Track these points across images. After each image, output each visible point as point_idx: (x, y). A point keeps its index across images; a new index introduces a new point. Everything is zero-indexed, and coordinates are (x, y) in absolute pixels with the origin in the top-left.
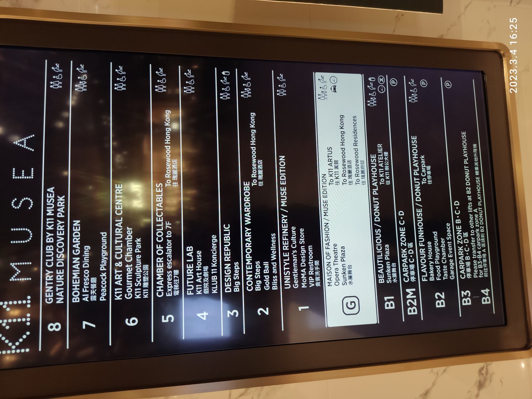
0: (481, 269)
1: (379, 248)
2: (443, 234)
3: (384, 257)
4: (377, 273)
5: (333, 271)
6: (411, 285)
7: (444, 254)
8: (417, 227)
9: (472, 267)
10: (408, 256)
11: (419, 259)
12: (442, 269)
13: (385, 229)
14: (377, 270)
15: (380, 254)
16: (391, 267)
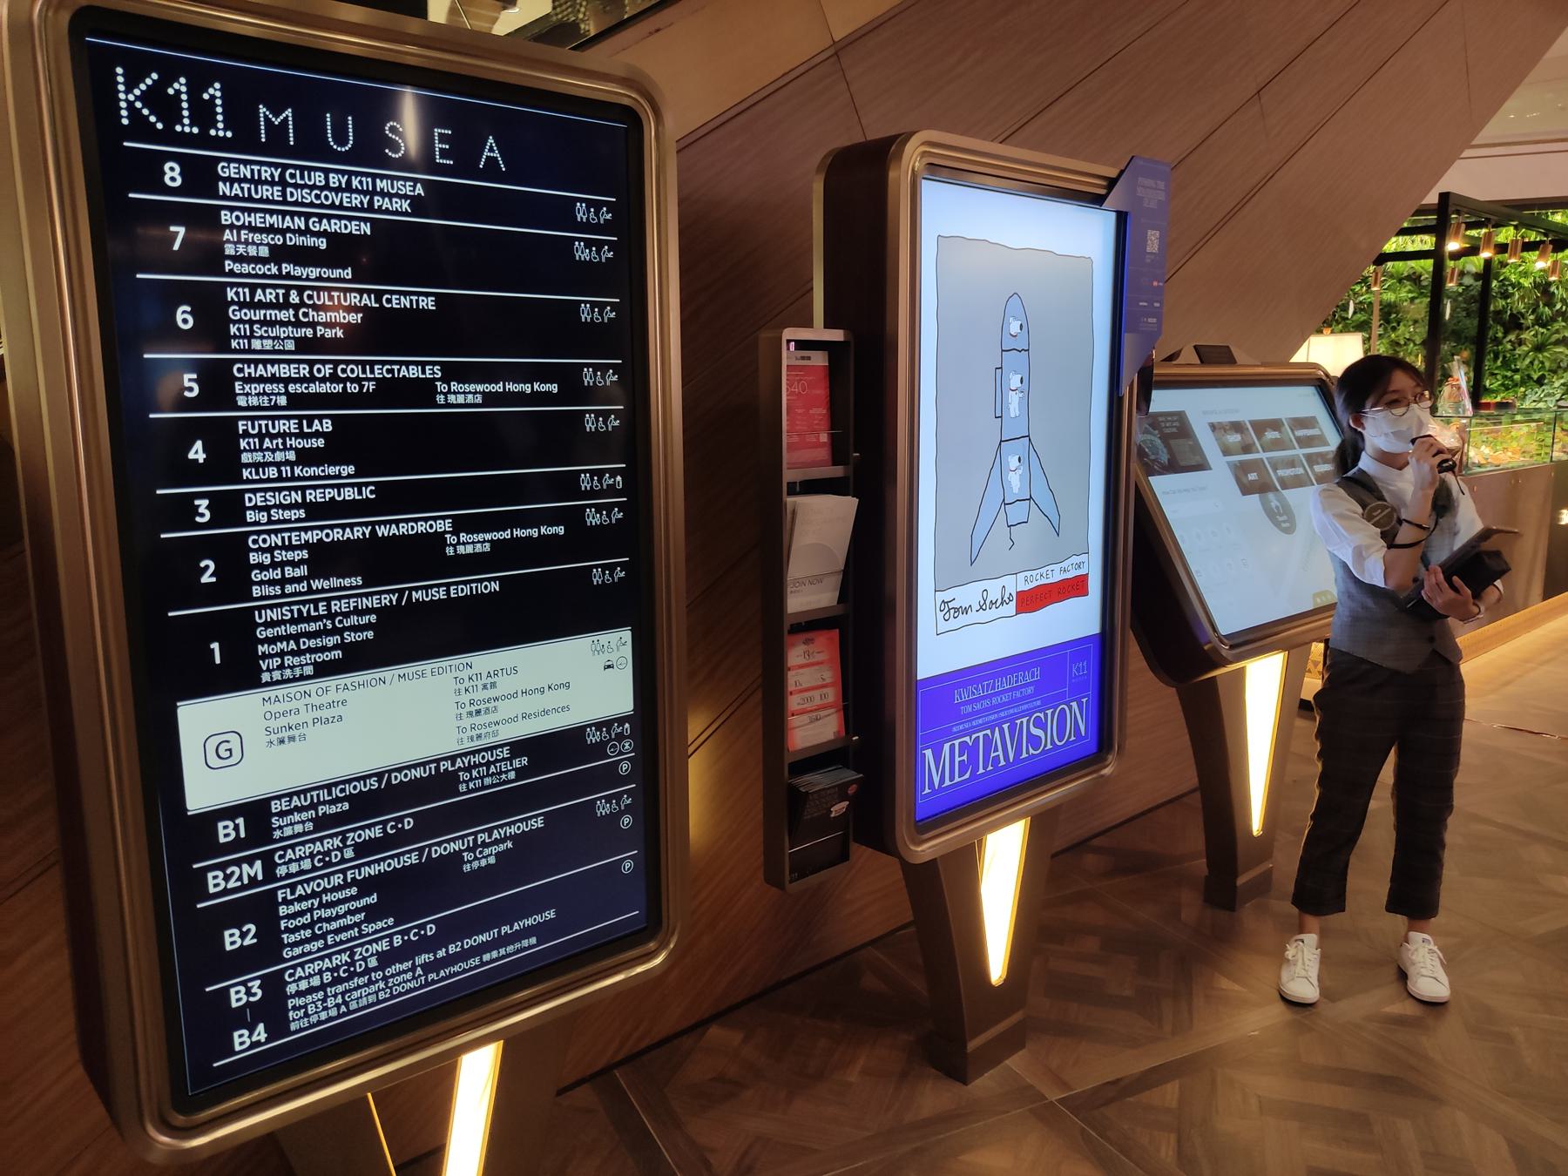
1: (342, 791)
2: (372, 914)
3: (324, 803)
4: (290, 795)
5: (294, 705)
8: (384, 859)
11: (322, 877)
14: (298, 793)
15: (330, 794)
16: (303, 822)
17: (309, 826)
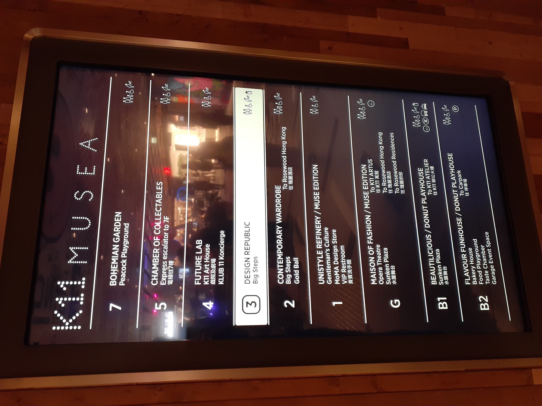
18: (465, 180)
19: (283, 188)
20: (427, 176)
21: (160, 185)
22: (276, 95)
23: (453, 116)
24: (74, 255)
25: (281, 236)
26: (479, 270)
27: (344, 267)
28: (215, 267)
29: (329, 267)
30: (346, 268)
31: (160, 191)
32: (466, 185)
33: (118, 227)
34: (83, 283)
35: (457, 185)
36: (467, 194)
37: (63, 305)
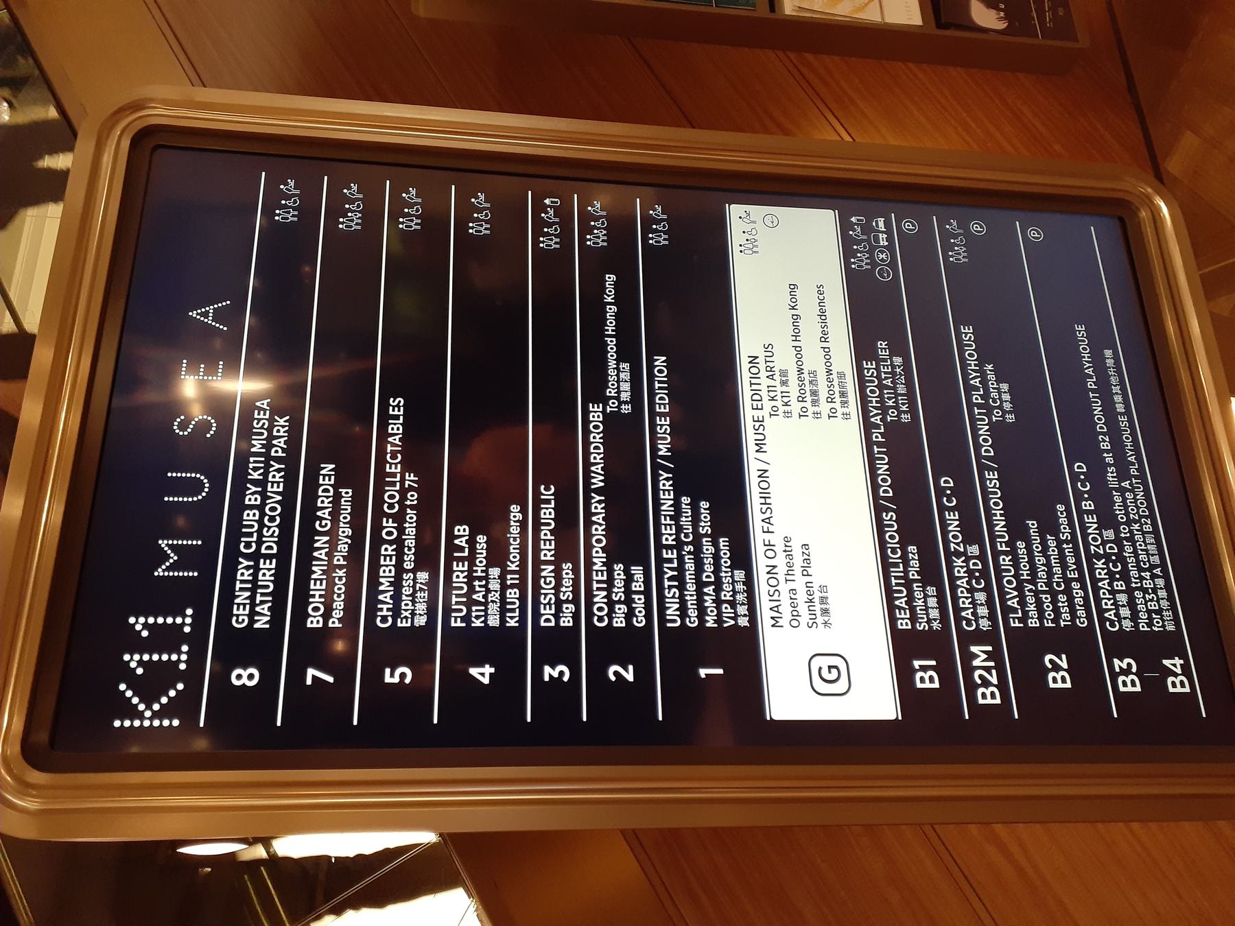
0: (1157, 612)
1: (894, 551)
3: (906, 572)
6: (979, 637)
7: (1057, 570)
9: (1132, 604)
10: (970, 573)
12: (1054, 601)
13: (905, 515)
15: (896, 565)
17: (931, 590)
18: (1005, 387)
19: (609, 409)
20: (886, 378)
21: (398, 405)
22: (477, 198)
23: (972, 242)
24: (169, 557)
25: (601, 516)
26: (1044, 592)
27: (727, 587)
28: (497, 587)
29: (691, 587)
30: (734, 590)
31: (397, 417)
32: (1006, 397)
33: (327, 497)
34: (188, 620)
35: (986, 396)
36: (1010, 418)
37: (140, 671)
